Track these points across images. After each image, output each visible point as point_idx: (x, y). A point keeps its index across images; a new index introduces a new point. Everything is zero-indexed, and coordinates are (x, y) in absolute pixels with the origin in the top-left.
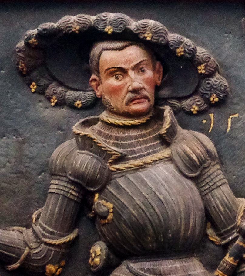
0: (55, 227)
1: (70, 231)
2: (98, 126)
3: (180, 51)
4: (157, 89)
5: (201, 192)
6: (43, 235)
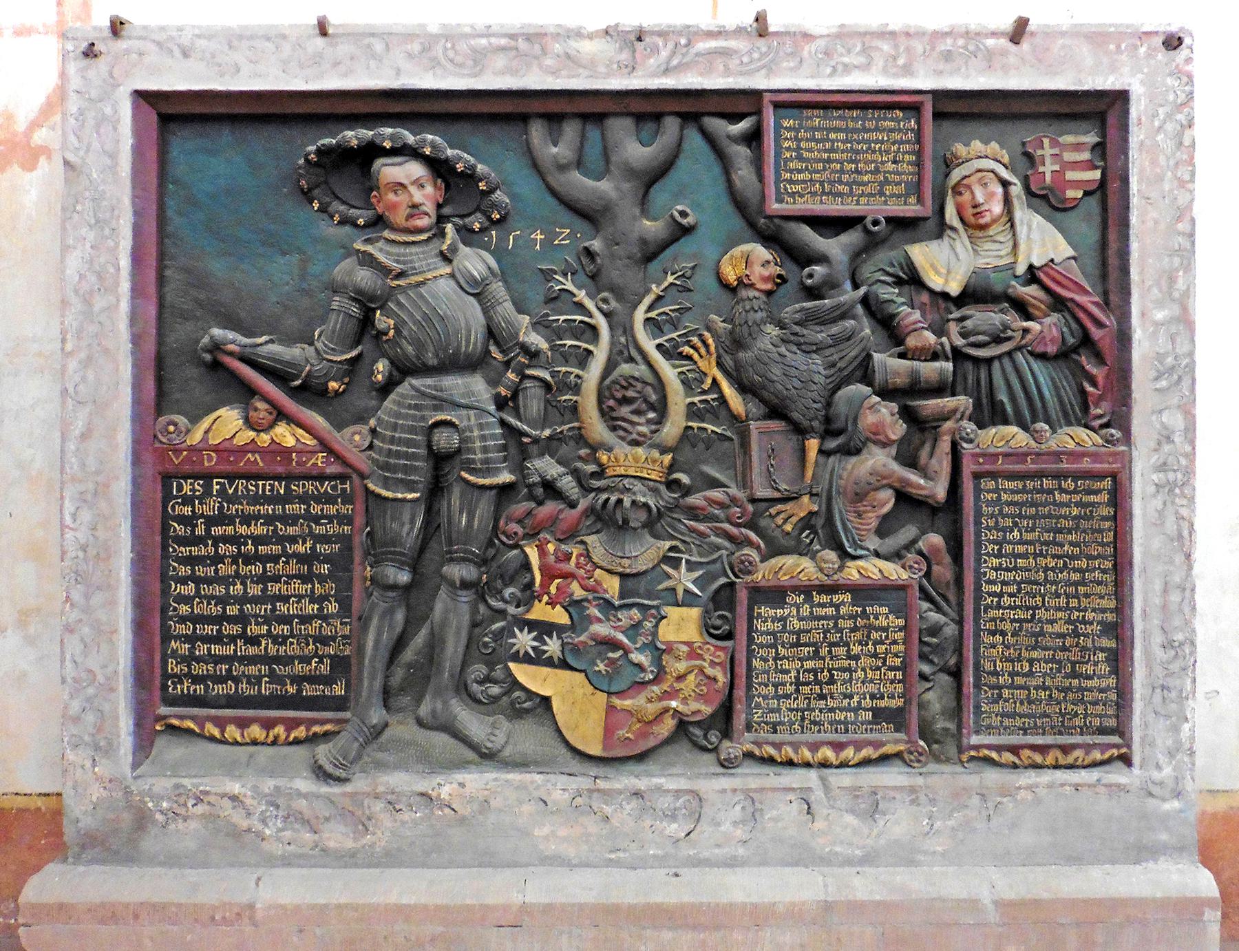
0: (336, 344)
1: (352, 348)
2: (380, 244)
3: (460, 167)
4: (439, 206)
5: (483, 309)
6: (325, 352)
